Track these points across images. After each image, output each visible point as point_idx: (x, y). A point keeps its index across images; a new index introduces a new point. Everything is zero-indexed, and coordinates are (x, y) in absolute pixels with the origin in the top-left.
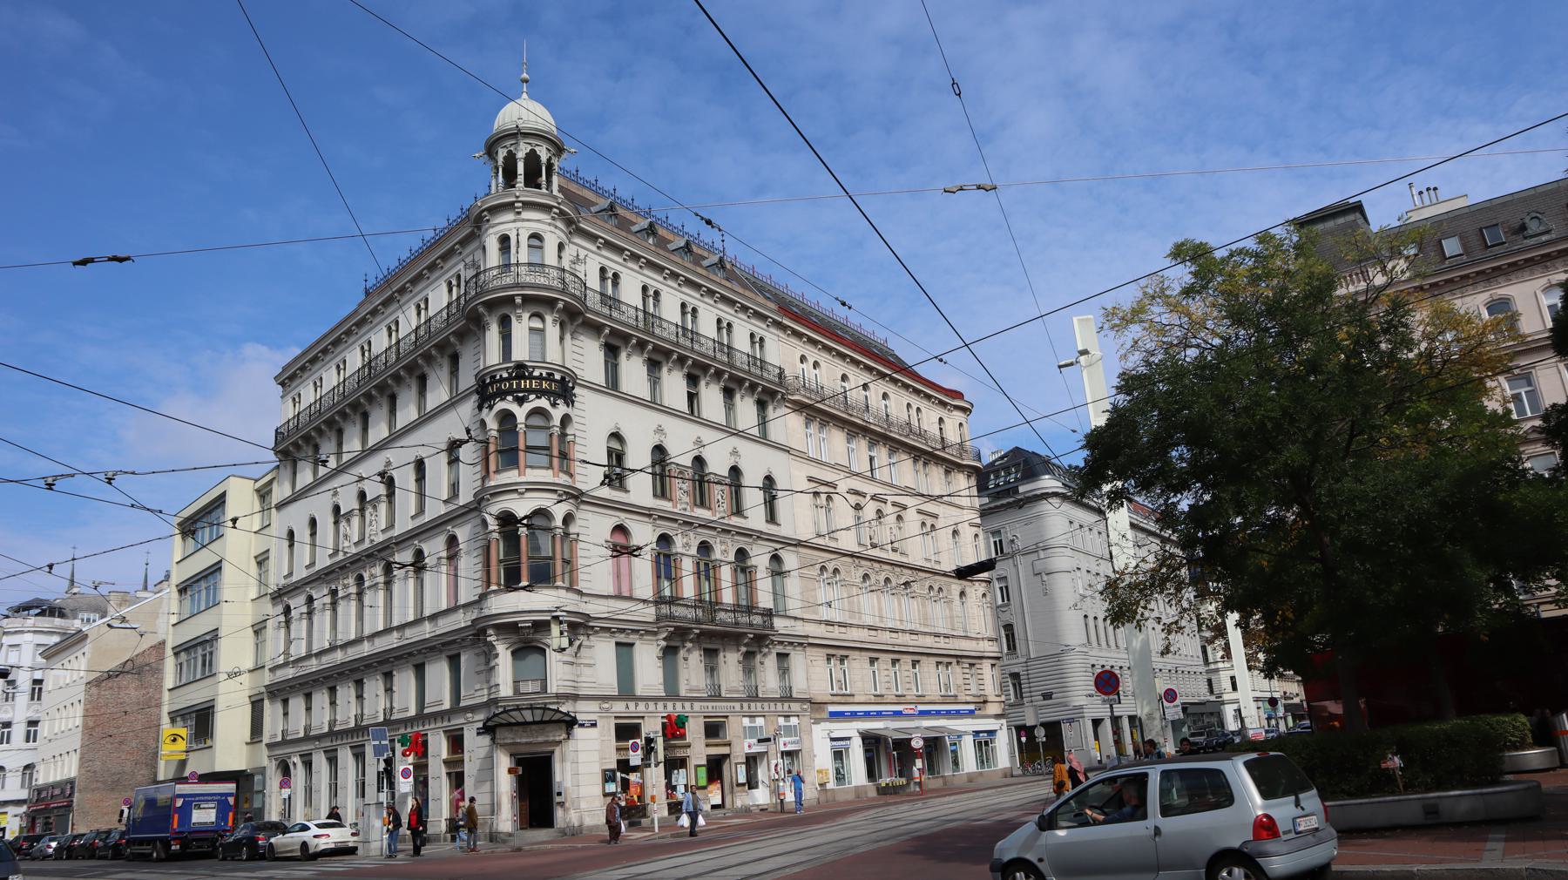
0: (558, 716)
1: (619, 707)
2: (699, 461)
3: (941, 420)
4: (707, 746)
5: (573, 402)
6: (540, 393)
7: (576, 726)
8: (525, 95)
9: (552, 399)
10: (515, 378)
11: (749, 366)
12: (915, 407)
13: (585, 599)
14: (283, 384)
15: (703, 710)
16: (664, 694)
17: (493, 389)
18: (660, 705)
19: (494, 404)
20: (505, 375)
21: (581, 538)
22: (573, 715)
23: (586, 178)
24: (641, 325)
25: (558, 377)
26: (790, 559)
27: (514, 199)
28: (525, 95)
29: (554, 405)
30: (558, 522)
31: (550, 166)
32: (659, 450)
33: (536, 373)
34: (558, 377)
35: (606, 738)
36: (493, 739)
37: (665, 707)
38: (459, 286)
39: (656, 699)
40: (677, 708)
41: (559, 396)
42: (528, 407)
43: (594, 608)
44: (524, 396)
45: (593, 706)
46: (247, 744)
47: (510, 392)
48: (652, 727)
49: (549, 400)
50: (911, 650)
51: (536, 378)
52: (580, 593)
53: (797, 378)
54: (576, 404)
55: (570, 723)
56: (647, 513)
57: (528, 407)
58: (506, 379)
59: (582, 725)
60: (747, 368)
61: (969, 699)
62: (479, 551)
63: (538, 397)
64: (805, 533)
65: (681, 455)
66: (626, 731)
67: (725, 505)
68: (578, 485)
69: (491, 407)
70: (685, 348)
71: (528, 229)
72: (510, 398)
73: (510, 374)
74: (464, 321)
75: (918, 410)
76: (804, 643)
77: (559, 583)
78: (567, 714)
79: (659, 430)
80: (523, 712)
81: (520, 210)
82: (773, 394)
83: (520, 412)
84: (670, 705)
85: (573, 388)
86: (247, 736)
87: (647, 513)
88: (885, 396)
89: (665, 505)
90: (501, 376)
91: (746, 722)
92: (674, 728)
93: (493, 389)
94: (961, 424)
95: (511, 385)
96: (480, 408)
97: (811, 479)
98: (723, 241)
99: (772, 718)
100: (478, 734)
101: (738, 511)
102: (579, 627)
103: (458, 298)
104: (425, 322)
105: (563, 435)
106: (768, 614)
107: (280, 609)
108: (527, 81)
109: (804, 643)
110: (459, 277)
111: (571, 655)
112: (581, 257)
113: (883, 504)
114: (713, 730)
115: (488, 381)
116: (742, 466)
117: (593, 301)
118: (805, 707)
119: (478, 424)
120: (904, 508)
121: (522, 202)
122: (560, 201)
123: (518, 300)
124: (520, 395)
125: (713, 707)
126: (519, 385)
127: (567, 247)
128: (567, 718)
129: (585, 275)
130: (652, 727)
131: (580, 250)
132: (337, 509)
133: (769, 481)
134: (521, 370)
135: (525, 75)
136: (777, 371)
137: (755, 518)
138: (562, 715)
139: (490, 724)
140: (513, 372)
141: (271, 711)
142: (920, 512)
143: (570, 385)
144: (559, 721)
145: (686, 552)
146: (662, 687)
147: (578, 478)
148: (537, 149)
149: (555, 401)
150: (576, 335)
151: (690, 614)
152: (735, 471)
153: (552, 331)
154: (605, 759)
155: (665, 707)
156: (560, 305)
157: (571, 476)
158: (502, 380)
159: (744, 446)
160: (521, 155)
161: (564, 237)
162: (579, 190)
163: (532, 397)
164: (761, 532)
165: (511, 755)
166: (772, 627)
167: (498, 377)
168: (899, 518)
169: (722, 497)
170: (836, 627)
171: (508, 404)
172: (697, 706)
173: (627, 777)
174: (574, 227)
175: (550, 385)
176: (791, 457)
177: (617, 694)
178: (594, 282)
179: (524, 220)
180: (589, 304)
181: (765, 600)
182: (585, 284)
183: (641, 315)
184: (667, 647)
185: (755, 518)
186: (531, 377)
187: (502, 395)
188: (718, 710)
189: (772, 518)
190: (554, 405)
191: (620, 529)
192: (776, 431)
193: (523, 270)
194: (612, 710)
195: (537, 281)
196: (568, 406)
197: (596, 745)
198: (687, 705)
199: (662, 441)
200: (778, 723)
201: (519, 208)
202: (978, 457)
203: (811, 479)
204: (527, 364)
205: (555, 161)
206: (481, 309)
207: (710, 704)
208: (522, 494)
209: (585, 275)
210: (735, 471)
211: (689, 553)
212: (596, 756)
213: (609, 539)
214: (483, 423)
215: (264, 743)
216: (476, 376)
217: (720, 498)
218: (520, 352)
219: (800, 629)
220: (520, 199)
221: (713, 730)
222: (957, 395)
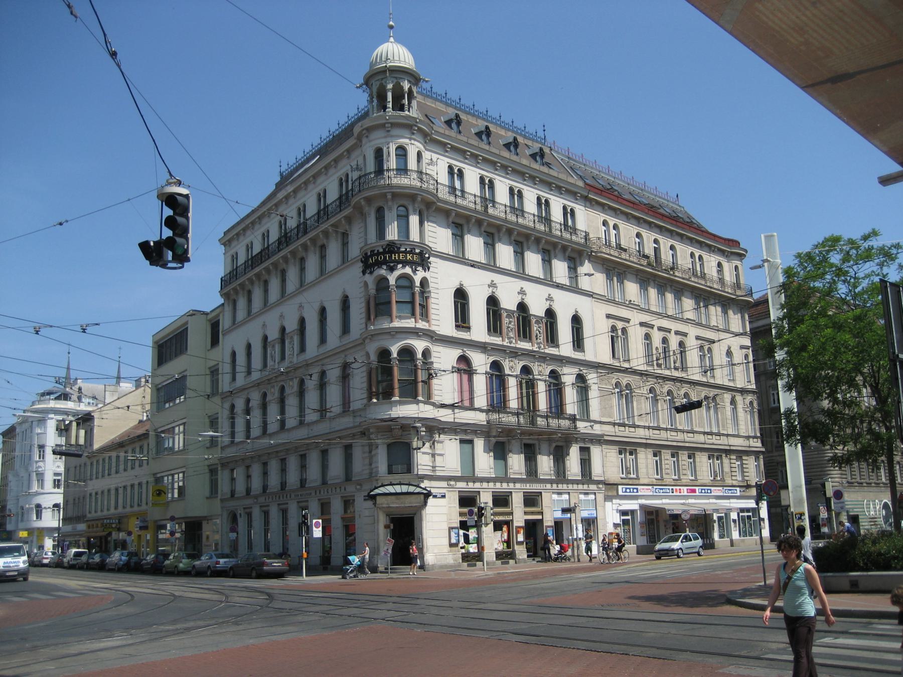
0: (418, 490)
1: (461, 485)
2: (522, 307)
3: (720, 265)
4: (526, 513)
5: (429, 268)
6: (405, 263)
7: (431, 497)
8: (392, 39)
10: (387, 253)
11: (561, 232)
14: (224, 244)
15: (522, 487)
17: (372, 261)
18: (491, 485)
19: (374, 271)
20: (381, 250)
22: (429, 489)
23: (439, 93)
24: (479, 207)
26: (592, 377)
27: (384, 121)
28: (392, 39)
29: (414, 271)
30: (419, 356)
31: (410, 92)
32: (492, 301)
34: (417, 251)
35: (452, 505)
36: (375, 504)
38: (347, 181)
39: (488, 480)
40: (504, 487)
41: (419, 265)
43: (445, 416)
44: (394, 266)
45: (444, 484)
46: (207, 498)
47: (385, 262)
48: (486, 499)
51: (403, 252)
52: (434, 404)
53: (599, 238)
54: (431, 269)
55: (428, 495)
56: (483, 347)
57: (397, 273)
58: (381, 253)
59: (435, 497)
60: (560, 234)
61: (735, 483)
62: (365, 374)
63: (404, 267)
65: (509, 302)
66: (467, 501)
67: (542, 338)
68: (433, 328)
69: (371, 273)
70: (511, 223)
72: (385, 267)
73: (384, 250)
74: (352, 210)
76: (599, 440)
77: (420, 398)
78: (425, 489)
79: (492, 285)
80: (395, 487)
81: (389, 129)
82: (580, 253)
83: (392, 279)
84: (498, 485)
85: (429, 258)
86: (207, 493)
87: (483, 347)
89: (497, 340)
90: (378, 251)
91: (555, 497)
92: (501, 500)
93: (372, 261)
94: (736, 267)
95: (385, 258)
96: (364, 273)
97: (609, 316)
98: (544, 130)
99: (574, 494)
100: (365, 500)
102: (434, 428)
103: (347, 192)
104: (324, 208)
105: (422, 293)
106: (573, 419)
107: (227, 405)
108: (391, 27)
109: (599, 440)
110: (347, 175)
112: (435, 160)
113: (668, 334)
114: (531, 500)
115: (369, 254)
116: (556, 308)
117: (443, 194)
118: (601, 486)
119: (362, 284)
120: (685, 335)
123: (389, 196)
124: (392, 264)
126: (390, 257)
127: (423, 153)
128: (425, 492)
129: (437, 174)
130: (486, 499)
131: (433, 154)
132: (265, 338)
133: (576, 320)
134: (392, 248)
135: (391, 23)
136: (584, 234)
137: (566, 348)
138: (421, 490)
139: (372, 493)
140: (386, 248)
141: (223, 478)
142: (698, 338)
143: (427, 256)
144: (419, 493)
145: (511, 374)
147: (433, 322)
151: (513, 420)
152: (550, 314)
153: (414, 220)
154: (451, 520)
157: (428, 321)
158: (379, 254)
159: (556, 293)
160: (390, 86)
161: (423, 148)
162: (432, 103)
163: (400, 266)
165: (387, 515)
166: (576, 427)
167: (376, 252)
169: (539, 332)
171: (383, 271)
172: (518, 486)
173: (467, 533)
175: (413, 257)
176: (594, 299)
177: (460, 475)
178: (444, 178)
180: (440, 195)
181: (571, 407)
182: (437, 181)
183: (478, 200)
184: (496, 442)
185: (566, 348)
187: (379, 264)
191: (463, 359)
192: (585, 283)
193: (392, 174)
194: (457, 486)
195: (402, 182)
196: (425, 271)
197: (445, 510)
198: (511, 485)
200: (579, 498)
201: (388, 128)
202: (751, 294)
203: (609, 316)
204: (397, 242)
205: (414, 89)
206: (363, 203)
208: (394, 335)
209: (437, 174)
210: (550, 314)
212: (445, 518)
213: (455, 365)
214: (366, 284)
215: (219, 498)
216: (361, 249)
218: (392, 233)
219: (598, 429)
221: (531, 500)
222: (735, 243)
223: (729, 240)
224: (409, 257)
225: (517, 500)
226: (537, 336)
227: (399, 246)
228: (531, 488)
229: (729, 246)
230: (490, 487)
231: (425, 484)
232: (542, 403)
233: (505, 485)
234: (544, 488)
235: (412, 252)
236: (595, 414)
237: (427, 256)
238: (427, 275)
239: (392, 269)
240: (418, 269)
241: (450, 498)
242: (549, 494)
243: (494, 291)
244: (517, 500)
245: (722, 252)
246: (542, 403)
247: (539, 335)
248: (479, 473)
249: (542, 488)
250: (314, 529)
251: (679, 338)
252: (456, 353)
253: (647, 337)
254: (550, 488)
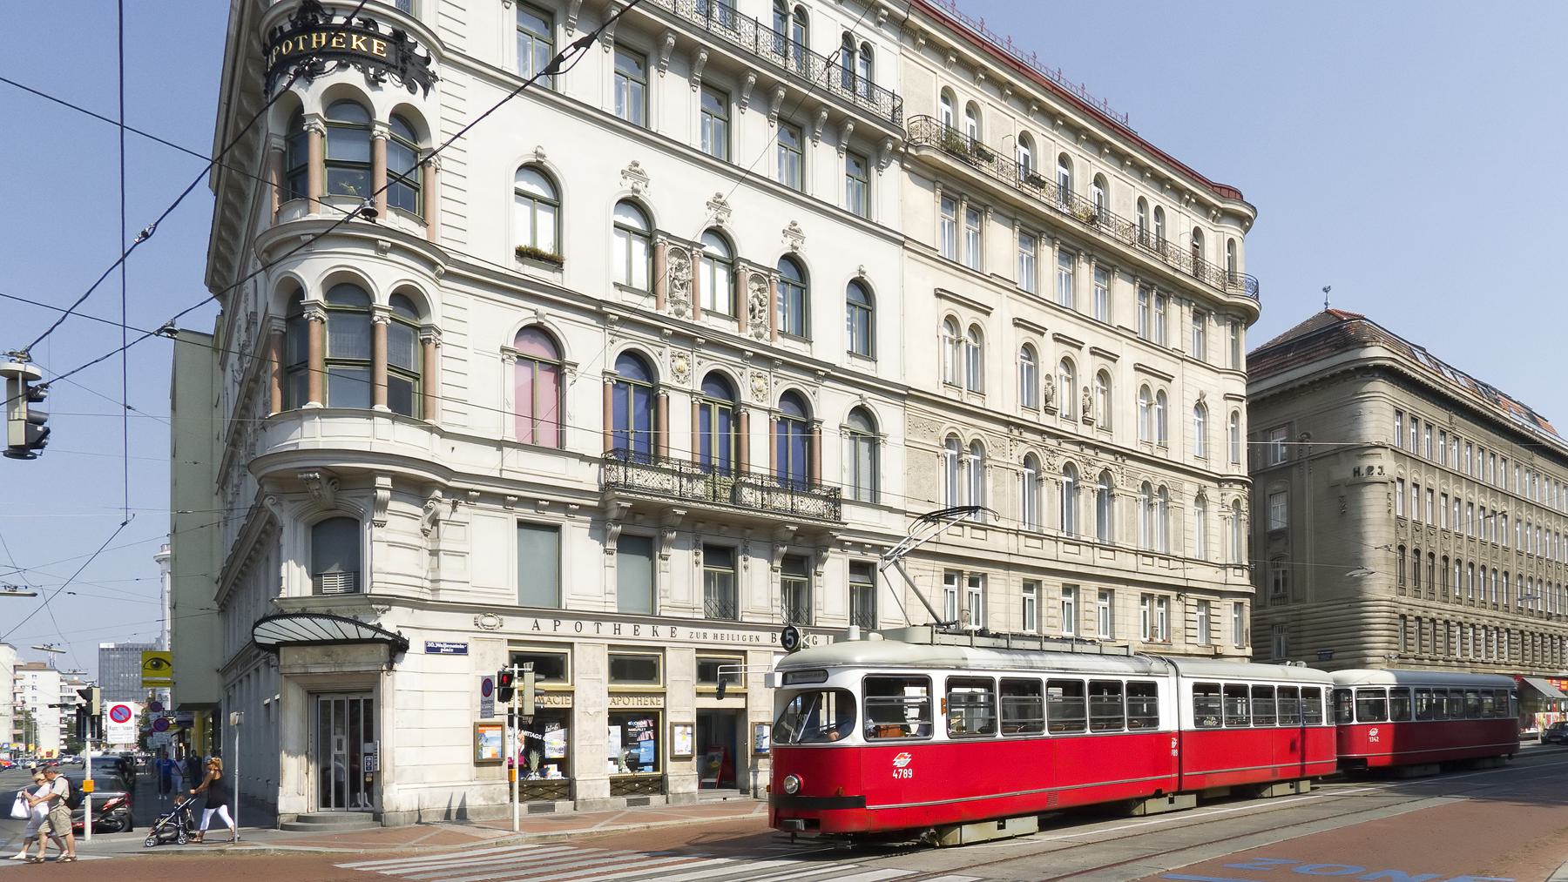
6: (347, 58)
10: (301, 32)
12: (1152, 206)
15: (695, 639)
16: (616, 610)
18: (607, 628)
33: (339, 20)
37: (617, 630)
39: (598, 618)
50: (1098, 572)
57: (322, 83)
64: (926, 380)
75: (1159, 212)
84: (627, 629)
88: (1099, 181)
101: (802, 330)
113: (1075, 351)
120: (1113, 358)
125: (716, 636)
126: (308, 43)
146: (613, 598)
155: (617, 630)
163: (331, 64)
164: (833, 367)
168: (1103, 375)
170: (967, 529)
172: (683, 633)
188: (725, 641)
189: (867, 348)
198: (664, 631)
199: (638, 192)
207: (710, 632)
223: (1221, 187)
225: (679, 669)
226: (752, 310)
227: (329, 12)
228: (719, 640)
229: (1223, 198)
230: (602, 634)
231: (391, 621)
232: (760, 454)
233: (646, 630)
234: (754, 642)
236: (893, 487)
239: (310, 75)
241: (482, 655)
242: (768, 655)
243: (636, 186)
244: (679, 669)
245: (1204, 207)
246: (760, 454)
247: (758, 308)
248: (570, 602)
249: (748, 642)
251: (1100, 363)
252: (521, 314)
253: (1029, 349)
254: (770, 643)
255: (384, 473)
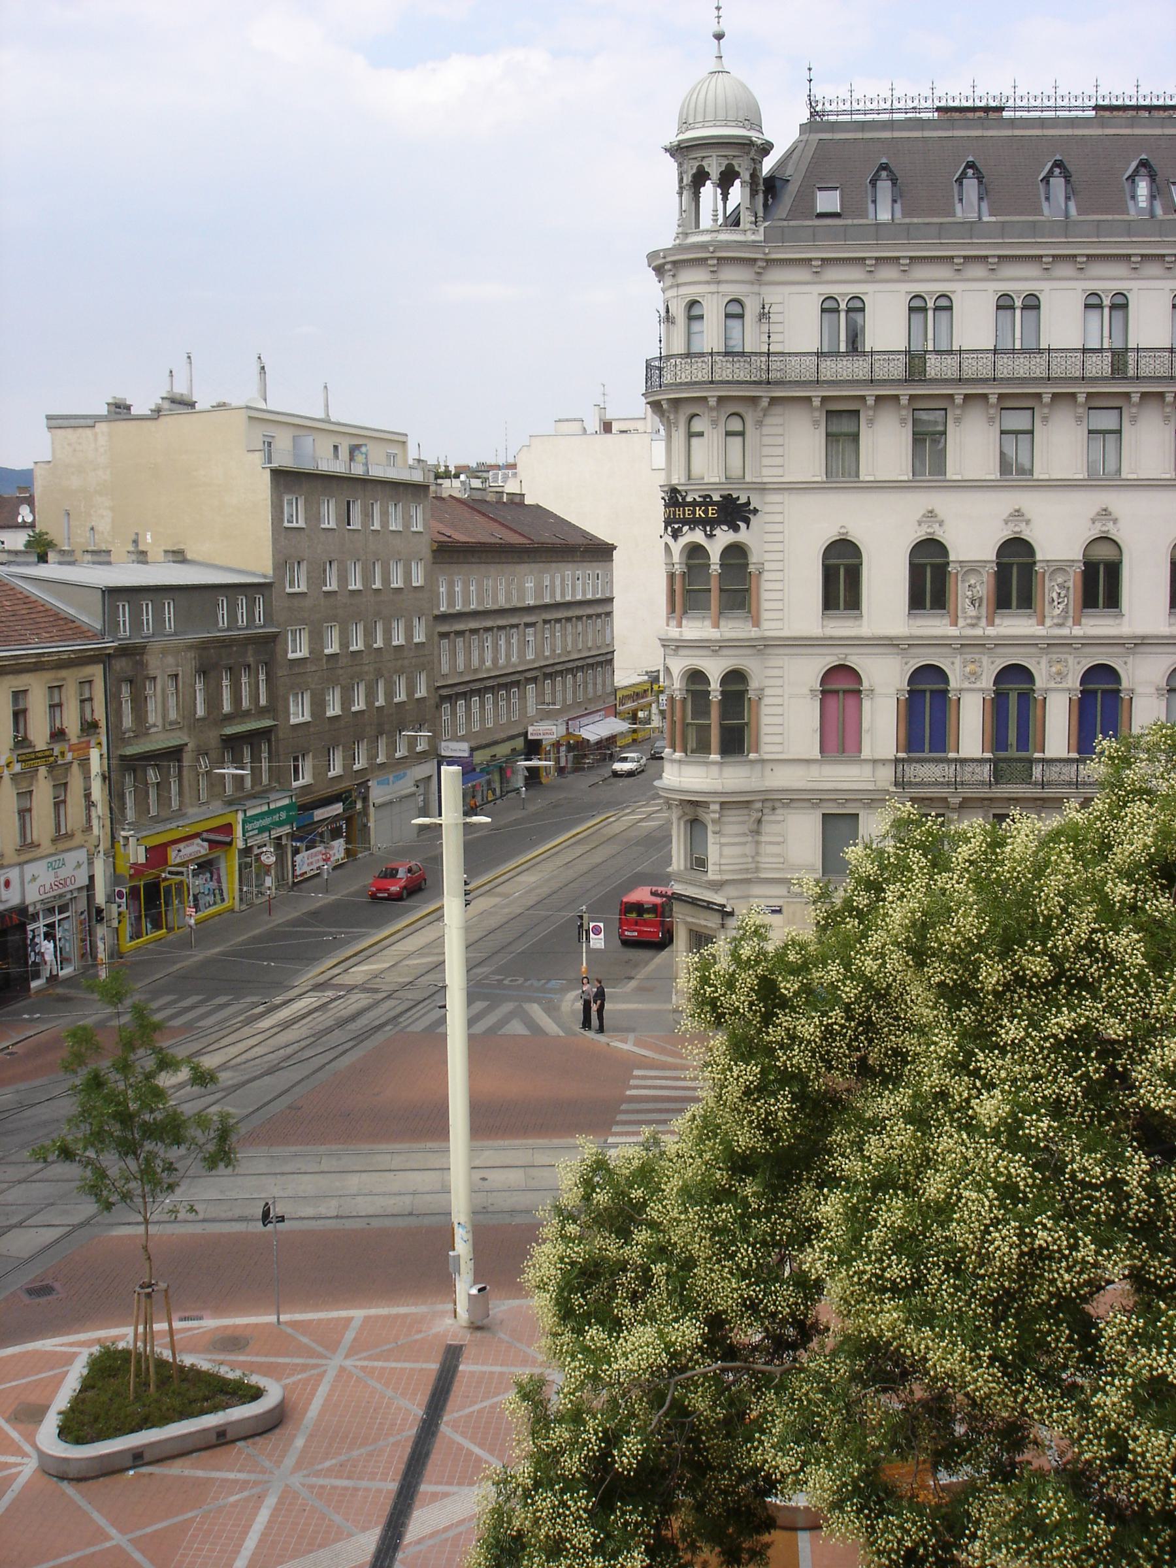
5: (747, 522)
6: (694, 523)
9: (708, 528)
13: (768, 767)
21: (768, 692)
25: (716, 498)
27: (662, 261)
29: (711, 536)
30: (715, 686)
33: (689, 499)
42: (683, 541)
49: (705, 531)
57: (683, 541)
71: (683, 296)
111: (745, 834)
121: (674, 263)
122: (711, 249)
148: (704, 163)
149: (711, 531)
150: (769, 420)
156: (712, 402)
163: (686, 528)
174: (760, 264)
175: (706, 512)
179: (678, 286)
186: (685, 504)
190: (711, 536)
196: (736, 529)
211: (978, 685)
217: (1055, 595)
220: (669, 259)
224: (699, 513)
235: (706, 501)
237: (743, 500)
238: (743, 536)
239: (676, 535)
240: (717, 532)
250: (592, 935)
255: (714, 802)
